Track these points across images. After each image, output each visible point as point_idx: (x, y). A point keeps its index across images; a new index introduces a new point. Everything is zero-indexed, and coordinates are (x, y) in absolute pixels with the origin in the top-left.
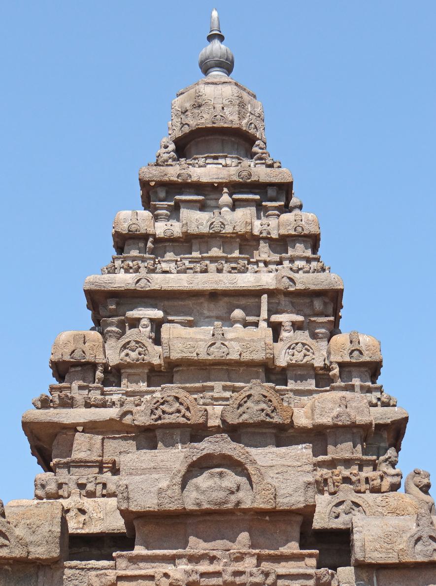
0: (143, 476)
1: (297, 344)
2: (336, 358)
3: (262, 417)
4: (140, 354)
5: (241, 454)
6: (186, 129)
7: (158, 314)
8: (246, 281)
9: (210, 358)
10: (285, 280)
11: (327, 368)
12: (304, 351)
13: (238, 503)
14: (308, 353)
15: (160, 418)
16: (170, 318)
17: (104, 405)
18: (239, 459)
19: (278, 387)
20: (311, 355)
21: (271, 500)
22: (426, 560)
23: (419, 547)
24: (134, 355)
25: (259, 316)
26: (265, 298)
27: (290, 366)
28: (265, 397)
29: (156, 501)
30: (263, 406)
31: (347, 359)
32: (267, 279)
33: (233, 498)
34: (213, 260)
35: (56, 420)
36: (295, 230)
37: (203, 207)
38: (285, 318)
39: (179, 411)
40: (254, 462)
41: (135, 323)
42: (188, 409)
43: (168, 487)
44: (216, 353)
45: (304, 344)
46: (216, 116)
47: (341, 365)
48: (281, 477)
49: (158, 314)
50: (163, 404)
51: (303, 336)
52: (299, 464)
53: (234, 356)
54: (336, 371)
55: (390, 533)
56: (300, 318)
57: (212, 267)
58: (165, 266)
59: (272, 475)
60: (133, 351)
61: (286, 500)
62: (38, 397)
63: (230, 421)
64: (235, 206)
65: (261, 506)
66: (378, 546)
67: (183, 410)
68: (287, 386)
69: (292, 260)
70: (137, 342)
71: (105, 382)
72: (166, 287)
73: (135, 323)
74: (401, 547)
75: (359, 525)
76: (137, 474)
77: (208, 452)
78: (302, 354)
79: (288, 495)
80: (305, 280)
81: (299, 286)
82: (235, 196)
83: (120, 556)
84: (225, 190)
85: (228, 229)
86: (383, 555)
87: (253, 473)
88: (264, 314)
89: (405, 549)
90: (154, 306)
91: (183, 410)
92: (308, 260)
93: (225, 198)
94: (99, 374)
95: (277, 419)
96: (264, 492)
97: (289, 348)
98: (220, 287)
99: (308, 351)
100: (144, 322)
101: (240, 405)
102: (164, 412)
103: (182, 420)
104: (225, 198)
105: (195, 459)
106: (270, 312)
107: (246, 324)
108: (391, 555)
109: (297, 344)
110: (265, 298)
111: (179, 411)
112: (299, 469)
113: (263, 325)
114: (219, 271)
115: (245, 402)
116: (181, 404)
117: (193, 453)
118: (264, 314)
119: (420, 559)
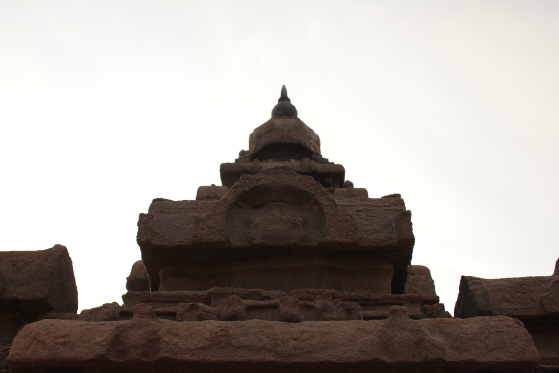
5: (308, 185)
6: (259, 148)
18: (307, 189)
21: (350, 233)
46: (283, 136)
48: (363, 214)
65: (337, 239)
66: (508, 296)
77: (266, 183)
79: (373, 232)
87: (325, 203)
89: (550, 296)
96: (340, 224)
105: (247, 189)
108: (530, 306)
112: (387, 208)
117: (245, 183)
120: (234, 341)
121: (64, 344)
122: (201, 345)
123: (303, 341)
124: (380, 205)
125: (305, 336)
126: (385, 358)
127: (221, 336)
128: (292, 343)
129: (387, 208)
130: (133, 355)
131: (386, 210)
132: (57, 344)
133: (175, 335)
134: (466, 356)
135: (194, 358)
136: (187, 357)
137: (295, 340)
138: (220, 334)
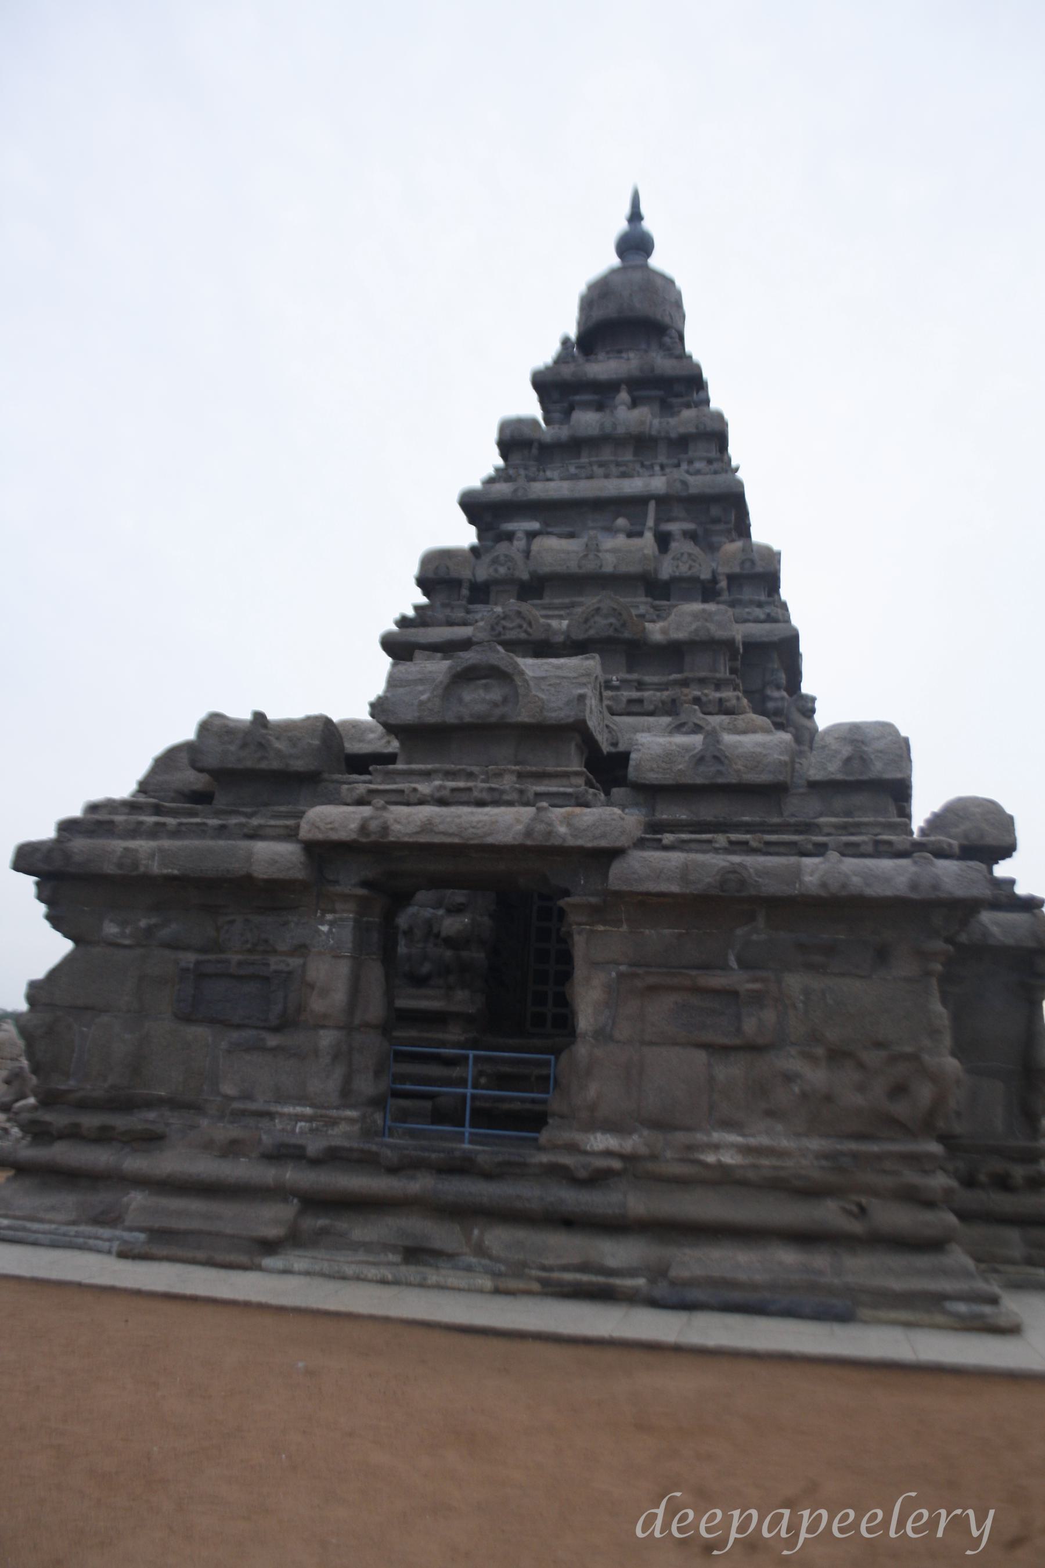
0: (407, 688)
1: (682, 554)
2: (723, 570)
3: (611, 632)
4: (509, 569)
7: (535, 525)
8: (634, 486)
9: (581, 571)
10: (678, 485)
11: (714, 580)
12: (690, 562)
13: (503, 716)
14: (694, 564)
15: (500, 634)
16: (550, 530)
17: (465, 624)
19: (657, 603)
20: (697, 566)
22: (706, 782)
23: (702, 769)
24: (502, 570)
25: (645, 525)
26: (652, 506)
27: (674, 580)
28: (614, 609)
29: (416, 714)
30: (612, 620)
31: (737, 570)
32: (658, 484)
33: (498, 712)
34: (601, 465)
35: (413, 639)
36: (697, 428)
37: (600, 407)
38: (674, 527)
39: (520, 626)
40: (522, 673)
41: (510, 536)
42: (530, 624)
43: (429, 699)
44: (590, 566)
45: (690, 555)
47: (731, 578)
49: (535, 525)
50: (504, 618)
51: (689, 547)
52: (575, 675)
53: (608, 569)
54: (723, 584)
55: (670, 752)
56: (690, 526)
57: (598, 471)
58: (549, 474)
59: (543, 687)
60: (502, 565)
61: (554, 715)
62: (397, 616)
63: (574, 636)
64: (634, 403)
66: (655, 766)
67: (525, 626)
68: (668, 600)
69: (690, 462)
70: (506, 556)
71: (472, 600)
72: (543, 495)
73: (510, 536)
74: (680, 767)
75: (639, 742)
76: (401, 686)
78: (687, 566)
80: (698, 484)
81: (693, 491)
82: (636, 394)
83: (376, 770)
84: (624, 386)
85: (621, 430)
86: (660, 776)
87: (520, 684)
88: (650, 522)
90: (535, 518)
91: (525, 626)
92: (710, 462)
93: (624, 396)
94: (465, 592)
95: (627, 635)
97: (673, 559)
98: (605, 494)
99: (694, 561)
100: (520, 534)
101: (586, 621)
102: (504, 628)
103: (523, 636)
104: (624, 396)
106: (658, 521)
107: (630, 535)
109: (682, 554)
110: (652, 506)
111: (520, 626)
112: (574, 681)
113: (649, 536)
114: (607, 476)
115: (593, 616)
116: (524, 618)
118: (650, 522)
119: (699, 781)
120: (435, 829)
121: (332, 829)
122: (415, 830)
123: (478, 828)
124: (570, 675)
125: (480, 825)
126: (529, 842)
127: (428, 824)
128: (471, 830)
129: (574, 681)
130: (373, 838)
131: (573, 683)
132: (327, 829)
133: (399, 823)
134: (580, 842)
135: (411, 840)
136: (406, 839)
137: (473, 827)
138: (427, 822)
